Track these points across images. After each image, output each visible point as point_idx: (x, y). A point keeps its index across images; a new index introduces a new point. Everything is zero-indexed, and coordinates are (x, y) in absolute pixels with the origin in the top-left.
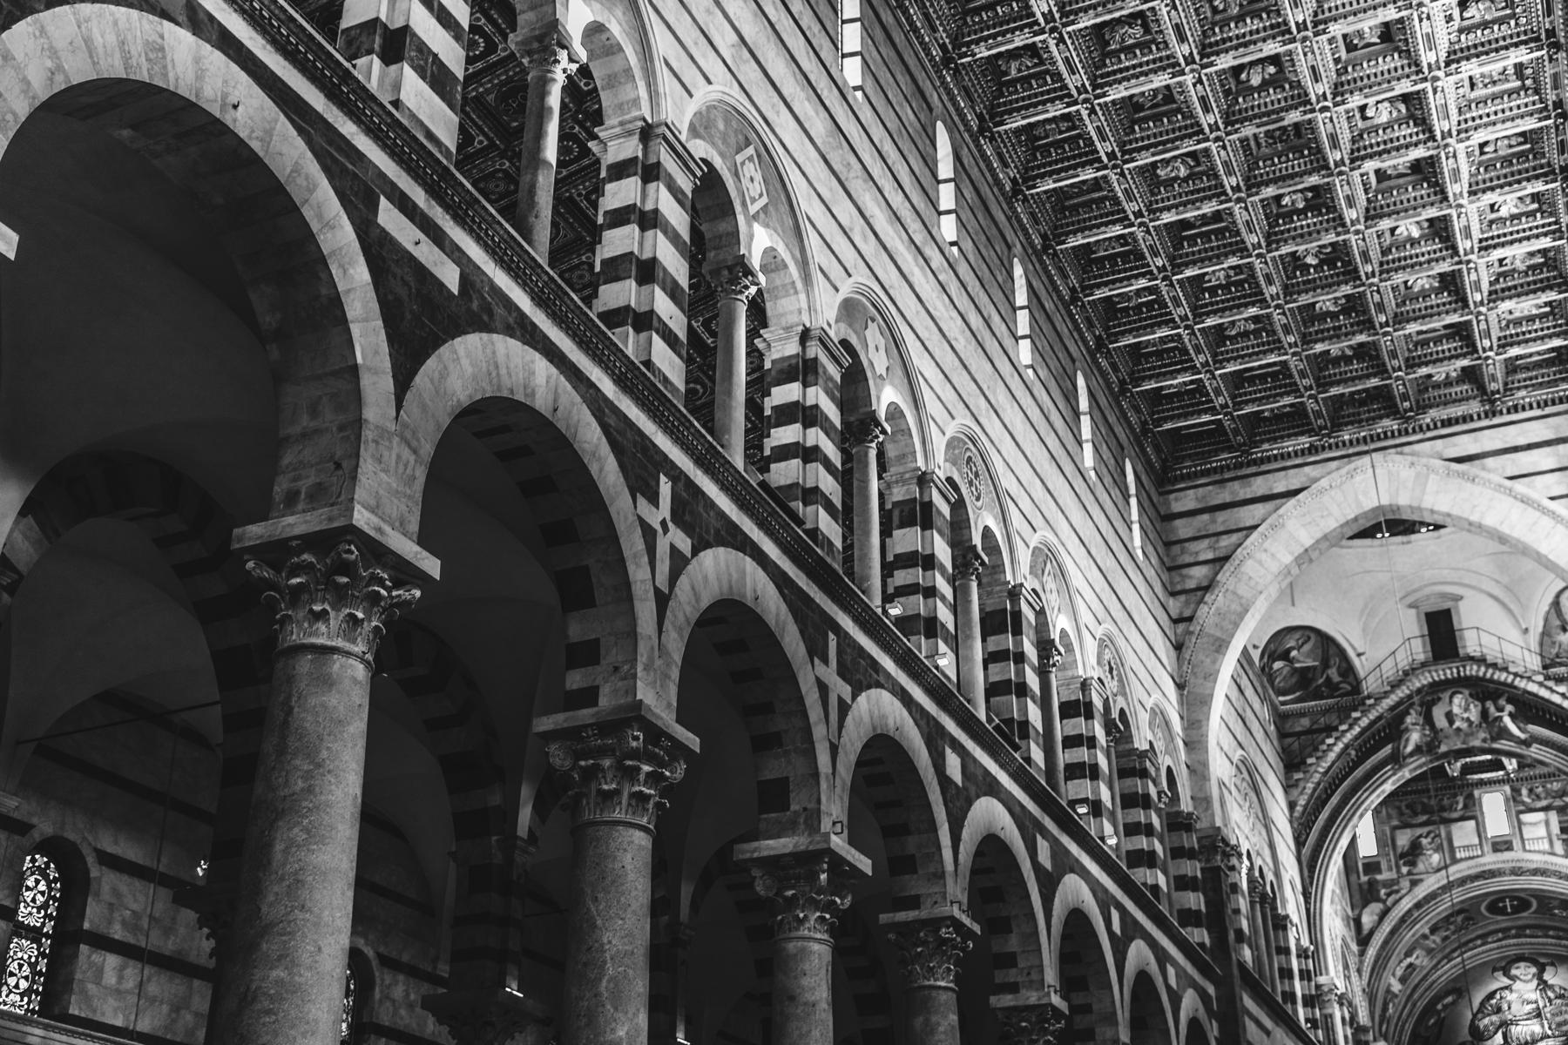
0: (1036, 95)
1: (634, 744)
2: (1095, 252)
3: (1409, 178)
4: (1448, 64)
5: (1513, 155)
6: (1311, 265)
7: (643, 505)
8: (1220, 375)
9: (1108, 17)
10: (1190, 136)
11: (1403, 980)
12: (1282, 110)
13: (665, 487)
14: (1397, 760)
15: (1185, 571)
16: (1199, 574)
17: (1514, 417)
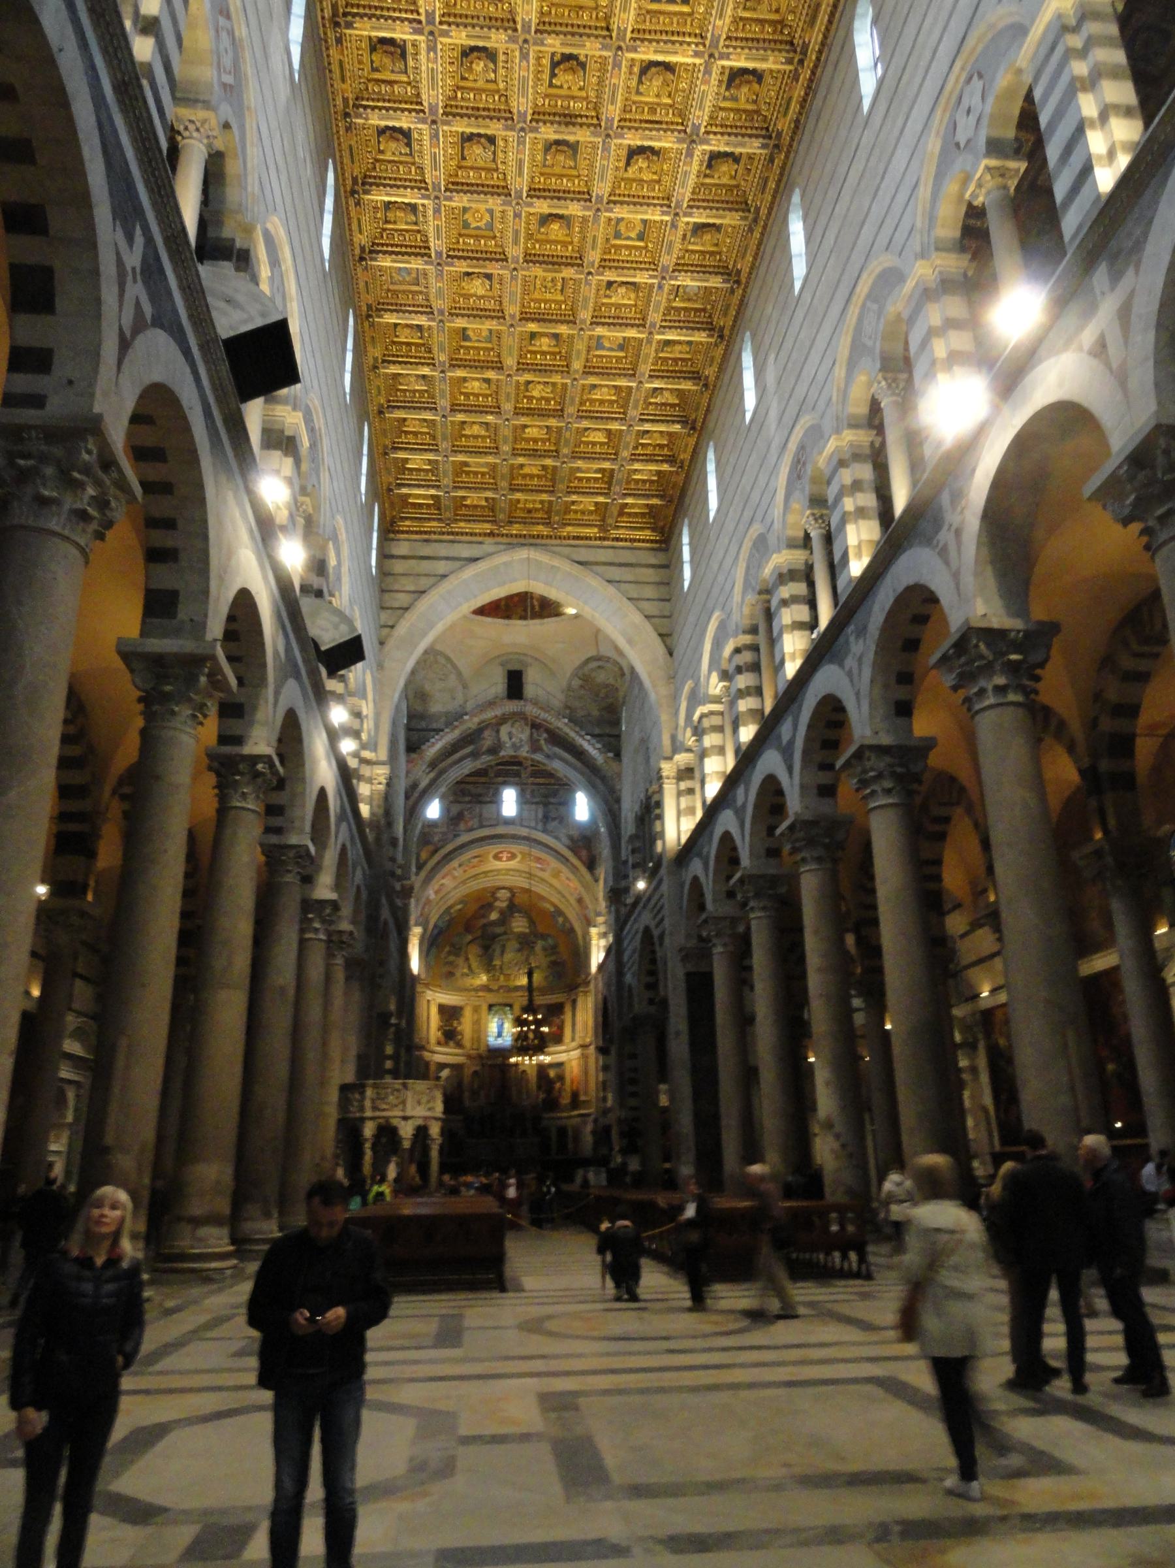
0: (400, 180)
1: (86, 457)
2: (397, 336)
3: (613, 354)
4: (674, 271)
5: (681, 359)
6: (533, 397)
7: (120, 235)
8: (453, 462)
9: (475, 131)
10: (497, 260)
11: (436, 892)
12: (563, 264)
13: (139, 239)
14: (475, 755)
15: (392, 594)
16: (402, 599)
17: (616, 544)
